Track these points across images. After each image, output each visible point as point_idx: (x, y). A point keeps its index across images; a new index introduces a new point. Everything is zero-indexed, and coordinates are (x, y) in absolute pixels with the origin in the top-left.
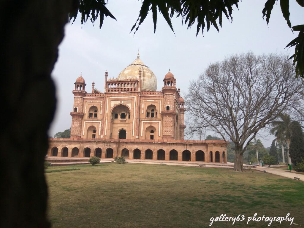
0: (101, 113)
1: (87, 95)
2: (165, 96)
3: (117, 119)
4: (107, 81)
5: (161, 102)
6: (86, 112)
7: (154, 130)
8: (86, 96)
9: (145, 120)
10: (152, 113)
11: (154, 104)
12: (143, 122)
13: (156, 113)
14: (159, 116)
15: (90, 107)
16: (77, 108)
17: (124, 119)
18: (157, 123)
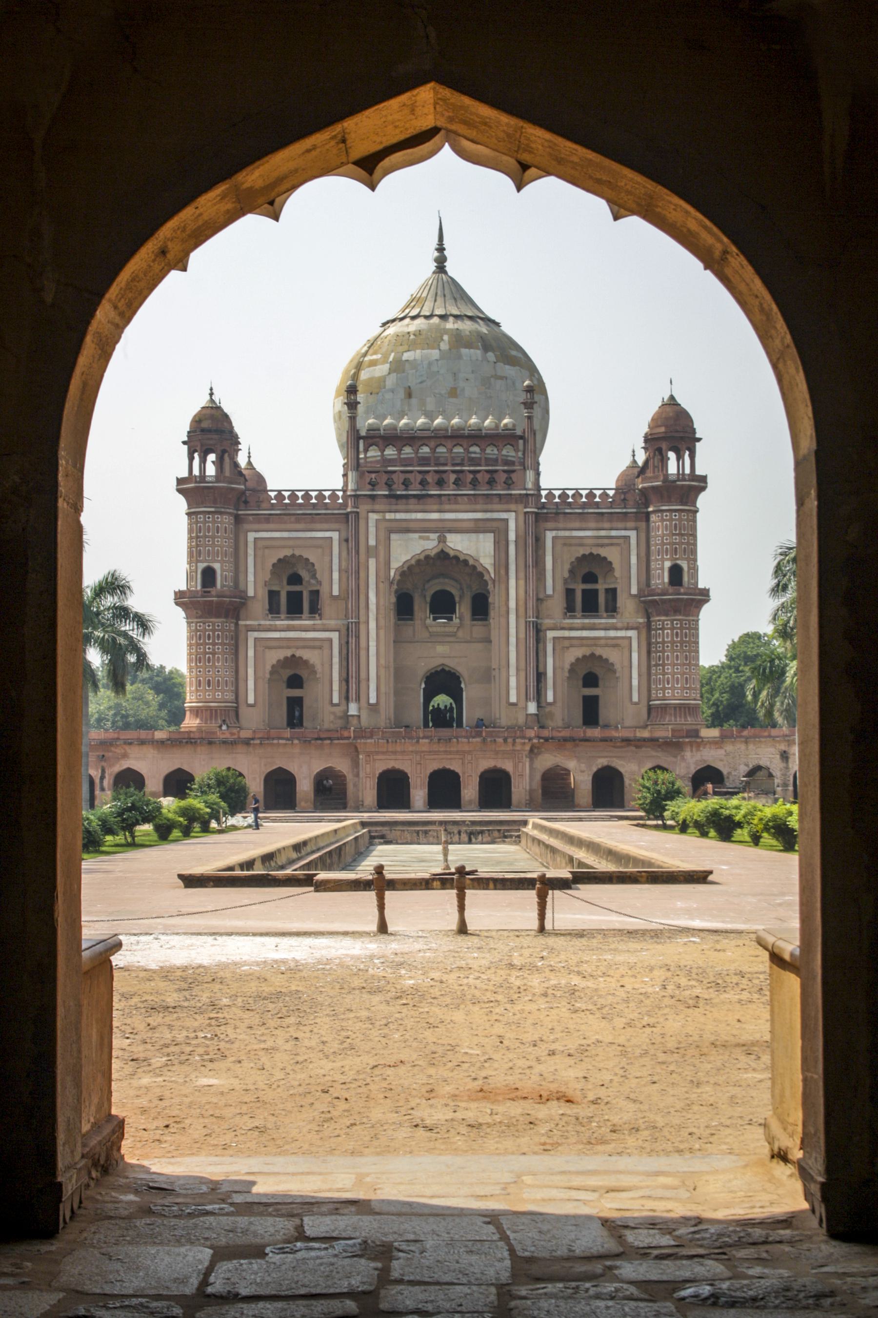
0: (336, 592)
2: (653, 518)
3: (412, 620)
4: (358, 431)
5: (633, 541)
6: (254, 584)
7: (599, 671)
8: (246, 502)
9: (562, 625)
10: (584, 591)
11: (603, 552)
12: (554, 638)
13: (612, 593)
14: (627, 606)
15: (275, 561)
16: (217, 566)
17: (450, 619)
18: (626, 642)
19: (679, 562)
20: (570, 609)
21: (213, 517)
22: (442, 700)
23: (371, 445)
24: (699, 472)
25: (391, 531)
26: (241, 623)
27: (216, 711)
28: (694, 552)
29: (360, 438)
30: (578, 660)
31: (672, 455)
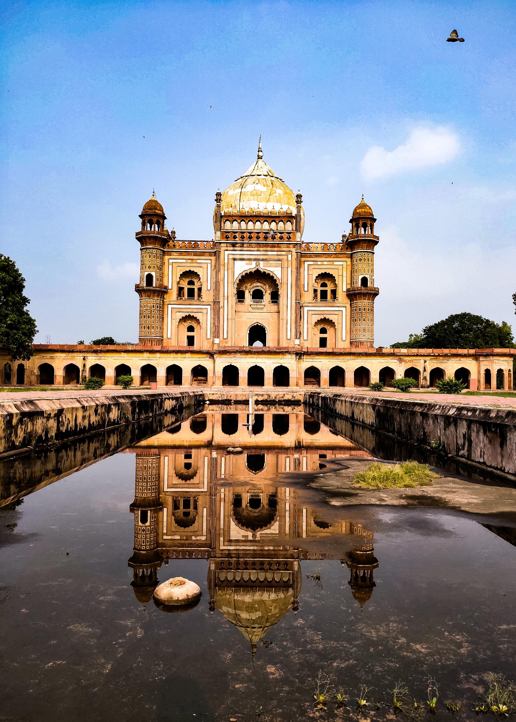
0: (209, 288)
1: (171, 243)
8: (168, 245)
10: (321, 290)
11: (331, 272)
16: (153, 274)
19: (366, 276)
20: (315, 296)
21: (152, 251)
22: (258, 344)
23: (226, 221)
24: (375, 234)
25: (234, 259)
26: (165, 301)
27: (152, 340)
28: (372, 271)
29: (222, 217)
30: (318, 321)
31: (363, 229)
